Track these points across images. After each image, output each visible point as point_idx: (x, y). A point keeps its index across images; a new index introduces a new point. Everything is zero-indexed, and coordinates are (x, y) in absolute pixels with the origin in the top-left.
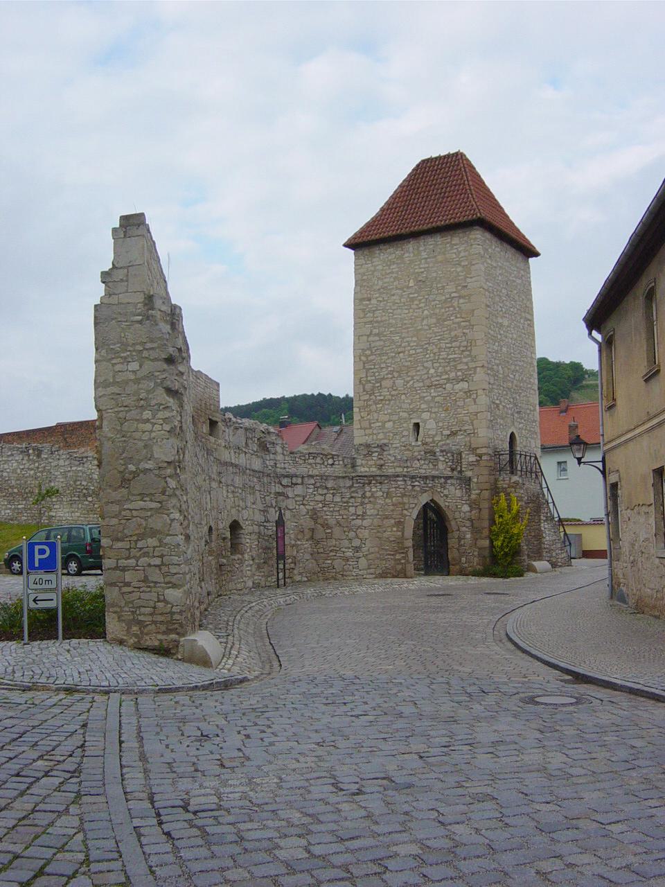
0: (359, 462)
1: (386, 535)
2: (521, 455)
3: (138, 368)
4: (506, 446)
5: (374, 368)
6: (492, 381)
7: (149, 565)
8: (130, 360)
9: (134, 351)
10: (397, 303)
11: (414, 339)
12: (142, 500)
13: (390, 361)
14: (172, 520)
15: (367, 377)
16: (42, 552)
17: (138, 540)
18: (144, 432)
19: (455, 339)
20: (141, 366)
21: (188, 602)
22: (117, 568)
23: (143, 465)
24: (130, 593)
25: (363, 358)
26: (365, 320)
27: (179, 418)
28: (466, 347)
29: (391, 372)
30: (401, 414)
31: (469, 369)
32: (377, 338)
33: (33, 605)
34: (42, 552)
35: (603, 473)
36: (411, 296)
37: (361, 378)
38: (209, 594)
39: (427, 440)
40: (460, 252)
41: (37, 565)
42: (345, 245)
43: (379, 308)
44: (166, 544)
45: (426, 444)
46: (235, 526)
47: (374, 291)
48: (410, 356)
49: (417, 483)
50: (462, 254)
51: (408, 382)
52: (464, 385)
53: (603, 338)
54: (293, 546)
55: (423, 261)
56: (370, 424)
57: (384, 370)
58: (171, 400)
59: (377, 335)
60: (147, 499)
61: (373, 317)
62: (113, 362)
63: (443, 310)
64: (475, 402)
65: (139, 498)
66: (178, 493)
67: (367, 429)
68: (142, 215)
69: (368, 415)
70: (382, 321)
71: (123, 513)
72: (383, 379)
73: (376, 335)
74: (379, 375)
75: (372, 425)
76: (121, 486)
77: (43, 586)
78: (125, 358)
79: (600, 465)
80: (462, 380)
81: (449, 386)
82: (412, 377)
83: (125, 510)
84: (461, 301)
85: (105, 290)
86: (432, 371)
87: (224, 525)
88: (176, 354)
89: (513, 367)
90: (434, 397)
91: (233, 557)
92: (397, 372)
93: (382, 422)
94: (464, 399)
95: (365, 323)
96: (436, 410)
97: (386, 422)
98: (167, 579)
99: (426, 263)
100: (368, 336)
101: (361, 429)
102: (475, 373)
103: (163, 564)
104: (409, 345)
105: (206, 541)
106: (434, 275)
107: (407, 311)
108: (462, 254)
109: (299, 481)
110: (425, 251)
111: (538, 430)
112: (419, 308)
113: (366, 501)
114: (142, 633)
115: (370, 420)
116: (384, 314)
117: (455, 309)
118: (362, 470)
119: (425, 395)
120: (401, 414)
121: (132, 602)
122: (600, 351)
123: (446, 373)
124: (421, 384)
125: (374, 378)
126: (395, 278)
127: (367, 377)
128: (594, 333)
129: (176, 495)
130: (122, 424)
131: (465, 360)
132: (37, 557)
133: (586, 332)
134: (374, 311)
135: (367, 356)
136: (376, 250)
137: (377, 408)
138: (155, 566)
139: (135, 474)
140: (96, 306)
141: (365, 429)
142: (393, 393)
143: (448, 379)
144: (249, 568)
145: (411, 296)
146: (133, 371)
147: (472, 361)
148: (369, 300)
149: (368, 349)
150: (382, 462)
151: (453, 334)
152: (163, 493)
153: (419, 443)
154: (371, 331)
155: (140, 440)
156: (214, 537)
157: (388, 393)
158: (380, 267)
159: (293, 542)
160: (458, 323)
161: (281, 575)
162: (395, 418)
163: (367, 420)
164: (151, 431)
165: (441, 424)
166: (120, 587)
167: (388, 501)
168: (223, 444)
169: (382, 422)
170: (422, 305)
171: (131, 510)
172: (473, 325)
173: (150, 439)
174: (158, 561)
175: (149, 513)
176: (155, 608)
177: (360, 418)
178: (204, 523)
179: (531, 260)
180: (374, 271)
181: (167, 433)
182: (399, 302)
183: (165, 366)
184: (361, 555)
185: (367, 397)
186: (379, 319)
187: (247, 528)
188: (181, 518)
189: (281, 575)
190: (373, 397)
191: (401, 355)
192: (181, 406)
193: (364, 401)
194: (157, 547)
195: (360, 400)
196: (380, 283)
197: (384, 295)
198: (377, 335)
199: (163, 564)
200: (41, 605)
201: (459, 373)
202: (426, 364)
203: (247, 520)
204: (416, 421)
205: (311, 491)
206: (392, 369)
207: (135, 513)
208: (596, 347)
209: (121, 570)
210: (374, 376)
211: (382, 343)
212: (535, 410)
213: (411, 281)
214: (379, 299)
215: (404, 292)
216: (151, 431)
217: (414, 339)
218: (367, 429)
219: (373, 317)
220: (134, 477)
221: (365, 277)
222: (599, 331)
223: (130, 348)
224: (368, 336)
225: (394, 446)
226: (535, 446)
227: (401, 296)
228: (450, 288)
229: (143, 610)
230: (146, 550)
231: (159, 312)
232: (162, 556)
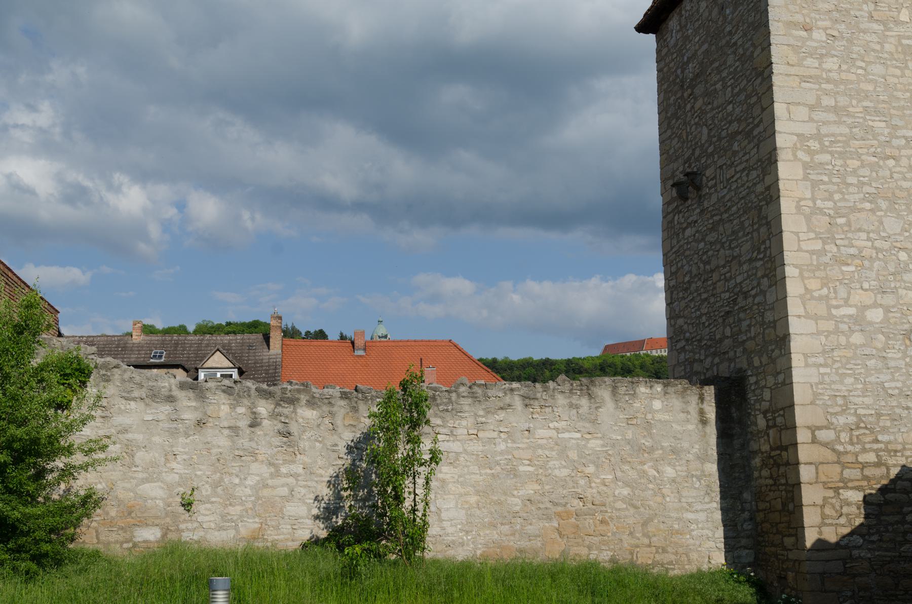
5: (831, 182)
10: (873, 50)
13: (866, 172)
15: (814, 199)
25: (801, 154)
29: (871, 198)
30: (902, 292)
32: (832, 117)
36: (905, 42)
37: (801, 200)
43: (833, 52)
47: (818, 11)
56: (829, 307)
57: (851, 189)
59: (835, 109)
61: (820, 68)
67: (822, 318)
69: (822, 288)
70: (842, 82)
72: (854, 209)
73: (827, 109)
74: (844, 199)
75: (834, 311)
92: (885, 198)
93: (856, 306)
95: (804, 79)
97: (866, 307)
101: (807, 316)
107: (898, 72)
116: (844, 67)
120: (902, 292)
125: (830, 204)
127: (814, 199)
134: (822, 55)
135: (811, 152)
137: (842, 272)
142: (878, 244)
145: (905, 42)
149: (812, 137)
154: (819, 99)
157: (870, 244)
162: (889, 300)
163: (820, 298)
169: (856, 306)
177: (802, 291)
182: (878, 47)
185: (818, 245)
186: (834, 75)
191: (891, 163)
193: (812, 252)
195: (800, 250)
197: (842, 27)
198: (835, 109)
206: (873, 190)
210: (830, 198)
214: (829, 32)
215: (889, 30)
218: (822, 318)
219: (820, 68)
224: (812, 108)
225: (892, 364)
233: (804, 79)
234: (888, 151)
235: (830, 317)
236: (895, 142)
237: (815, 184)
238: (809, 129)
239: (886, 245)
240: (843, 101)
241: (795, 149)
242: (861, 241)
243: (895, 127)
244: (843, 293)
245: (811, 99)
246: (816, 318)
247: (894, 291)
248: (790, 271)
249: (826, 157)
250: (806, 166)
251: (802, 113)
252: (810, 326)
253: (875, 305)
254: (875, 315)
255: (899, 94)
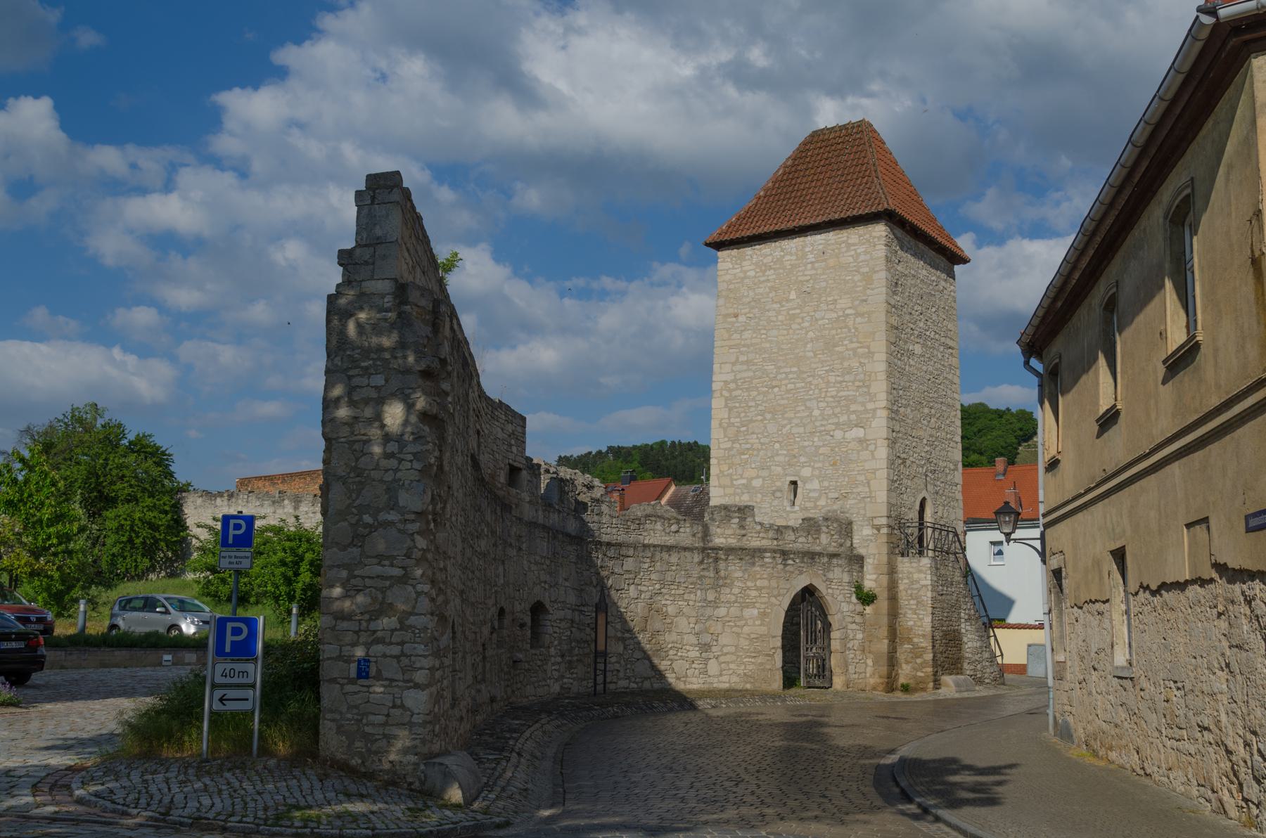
0: (714, 529)
1: (746, 629)
2: (934, 529)
3: (383, 382)
4: (914, 515)
6: (897, 428)
7: (385, 656)
8: (372, 371)
9: (379, 359)
11: (795, 369)
12: (379, 564)
13: (760, 397)
14: (419, 594)
16: (237, 631)
17: (370, 619)
18: (387, 471)
19: (849, 371)
20: (387, 381)
21: (436, 710)
22: (340, 657)
23: (383, 516)
24: (355, 693)
26: (732, 343)
27: (437, 453)
28: (863, 381)
29: (762, 413)
31: (866, 411)
32: (745, 367)
33: (217, 706)
34: (237, 631)
35: (1043, 555)
38: (493, 700)
39: (808, 505)
40: (858, 255)
41: (228, 649)
42: (707, 245)
44: (410, 626)
45: (806, 509)
46: (538, 609)
48: (788, 391)
49: (790, 562)
50: (862, 258)
51: (784, 426)
52: (859, 433)
53: (1045, 369)
54: (619, 639)
55: (809, 266)
56: (732, 480)
58: (427, 429)
60: (387, 563)
62: (351, 373)
63: (834, 332)
64: (873, 458)
65: (375, 561)
66: (430, 556)
68: (398, 173)
71: (353, 581)
73: (742, 363)
76: (352, 544)
77: (235, 680)
78: (367, 368)
79: (1037, 544)
80: (856, 426)
81: (838, 434)
82: (790, 420)
83: (355, 577)
84: (859, 320)
85: (343, 275)
86: (816, 413)
87: (521, 609)
88: (436, 364)
89: (926, 410)
90: (818, 448)
91: (533, 651)
94: (858, 452)
95: (731, 347)
96: (820, 465)
97: (752, 479)
98: (406, 677)
99: (813, 268)
100: (734, 364)
101: (720, 486)
102: (874, 417)
103: (403, 654)
104: (786, 378)
105: (493, 628)
106: (823, 284)
108: (862, 258)
109: (631, 552)
110: (811, 252)
111: (959, 496)
112: (802, 329)
113: (721, 582)
114: (369, 750)
115: (731, 475)
117: (850, 331)
118: (718, 541)
119: (806, 444)
121: (356, 707)
122: (1040, 386)
123: (835, 415)
124: (801, 430)
126: (772, 288)
128: (1034, 362)
129: (427, 560)
130: (357, 460)
131: (860, 399)
132: (229, 638)
133: (1022, 359)
135: (730, 391)
136: (748, 251)
138: (391, 656)
139: (372, 528)
140: (330, 297)
141: (724, 487)
143: (837, 424)
144: (556, 667)
146: (376, 387)
147: (871, 401)
148: (736, 316)
149: (733, 381)
150: (743, 532)
151: (846, 364)
152: (408, 556)
153: (797, 508)
155: (381, 481)
156: (507, 621)
158: (752, 273)
159: (619, 634)
160: (854, 350)
161: (600, 679)
162: (765, 473)
164: (396, 470)
165: (826, 484)
166: (342, 685)
167: (749, 584)
168: (528, 499)
170: (806, 324)
171: (363, 578)
172: (873, 353)
173: (395, 480)
174: (395, 650)
175: (388, 583)
176: (388, 715)
178: (491, 602)
179: (956, 268)
180: (743, 279)
181: (417, 473)
183: (420, 381)
184: (711, 655)
185: (729, 445)
186: (748, 342)
187: (555, 614)
188: (434, 593)
189: (600, 679)
190: (737, 445)
191: (776, 390)
192: (442, 438)
194: (396, 630)
196: (751, 294)
198: (747, 362)
199: (403, 654)
200: (231, 706)
201: (853, 417)
202: (808, 404)
203: (555, 601)
204: (793, 479)
205: (646, 566)
207: (368, 582)
208: (1035, 380)
209: (346, 661)
210: (739, 417)
211: (751, 374)
212: (956, 469)
213: (793, 292)
216: (396, 470)
217: (795, 369)
220: (371, 532)
221: (732, 286)
222: (1040, 357)
223: (373, 356)
224: (734, 364)
226: (956, 516)
227: (778, 313)
228: (844, 302)
229: (371, 718)
230: (379, 634)
231: (416, 309)
232: (402, 643)
233: (731, 347)
234: (774, 383)
235: (732, 485)
236: (779, 377)
237: (730, 410)
238: (730, 377)
239: (767, 440)
240: (751, 356)
241: (721, 390)
242: (753, 439)
243: (780, 367)
244: (740, 471)
245: (733, 359)
246: (724, 487)
247: (769, 468)
248: (713, 461)
249: (739, 392)
250: (727, 399)
251: (727, 368)
252: (721, 492)
253: (758, 477)
254: (757, 483)
255: (784, 347)
